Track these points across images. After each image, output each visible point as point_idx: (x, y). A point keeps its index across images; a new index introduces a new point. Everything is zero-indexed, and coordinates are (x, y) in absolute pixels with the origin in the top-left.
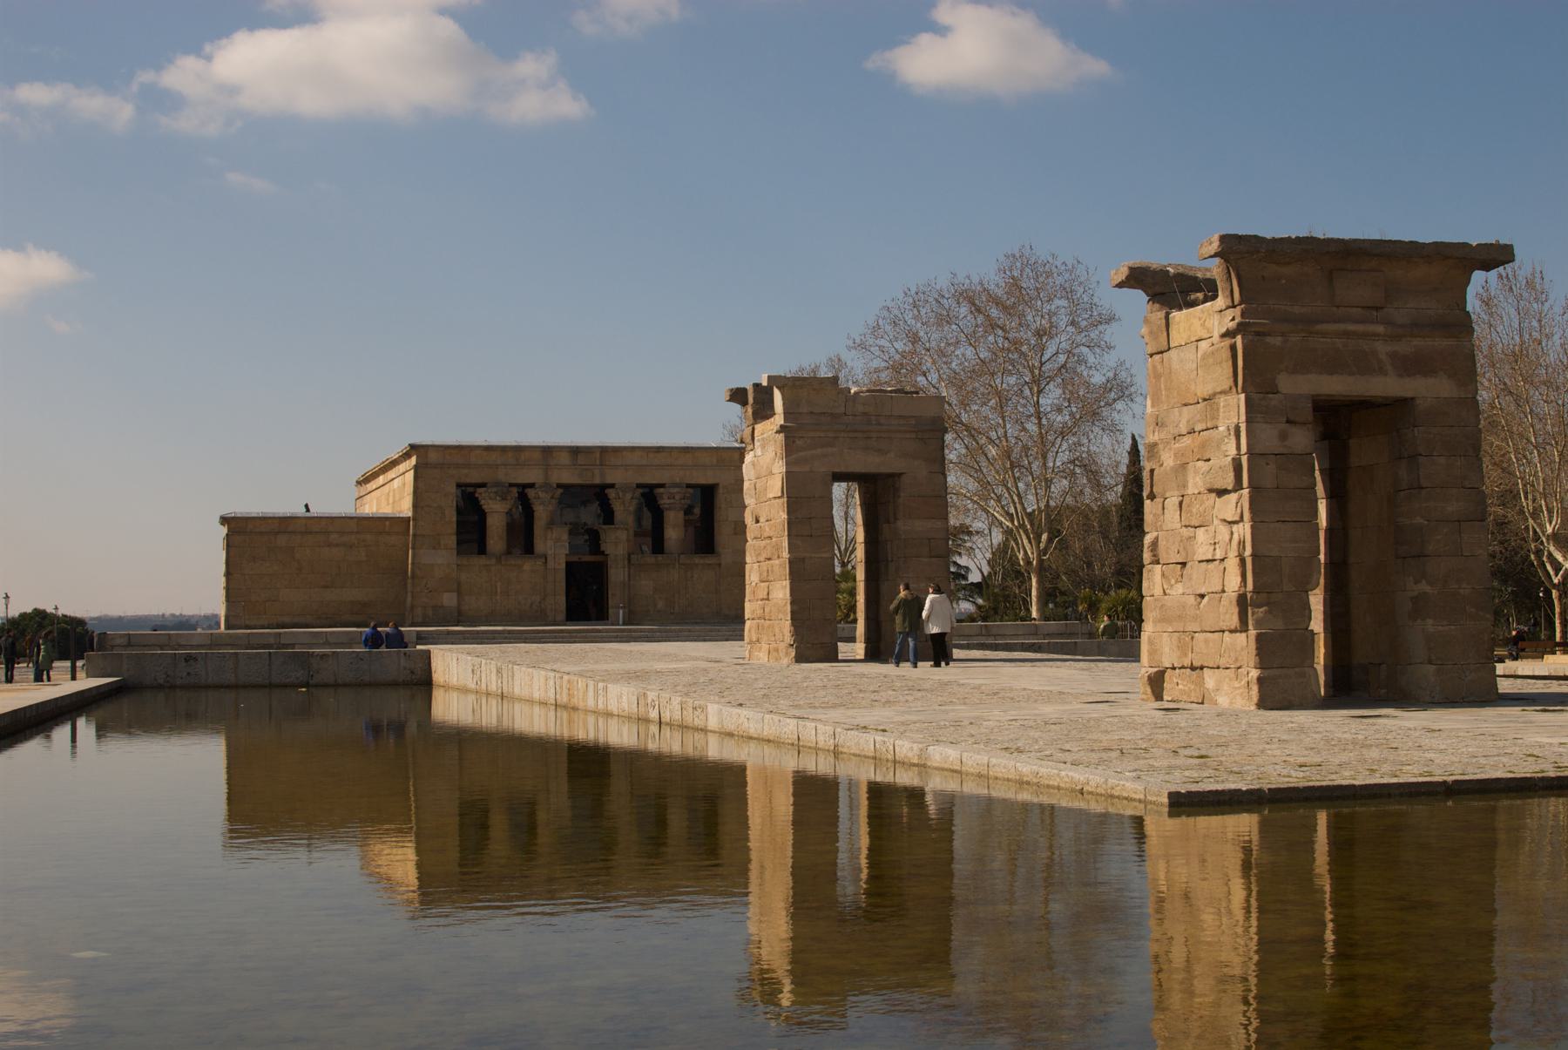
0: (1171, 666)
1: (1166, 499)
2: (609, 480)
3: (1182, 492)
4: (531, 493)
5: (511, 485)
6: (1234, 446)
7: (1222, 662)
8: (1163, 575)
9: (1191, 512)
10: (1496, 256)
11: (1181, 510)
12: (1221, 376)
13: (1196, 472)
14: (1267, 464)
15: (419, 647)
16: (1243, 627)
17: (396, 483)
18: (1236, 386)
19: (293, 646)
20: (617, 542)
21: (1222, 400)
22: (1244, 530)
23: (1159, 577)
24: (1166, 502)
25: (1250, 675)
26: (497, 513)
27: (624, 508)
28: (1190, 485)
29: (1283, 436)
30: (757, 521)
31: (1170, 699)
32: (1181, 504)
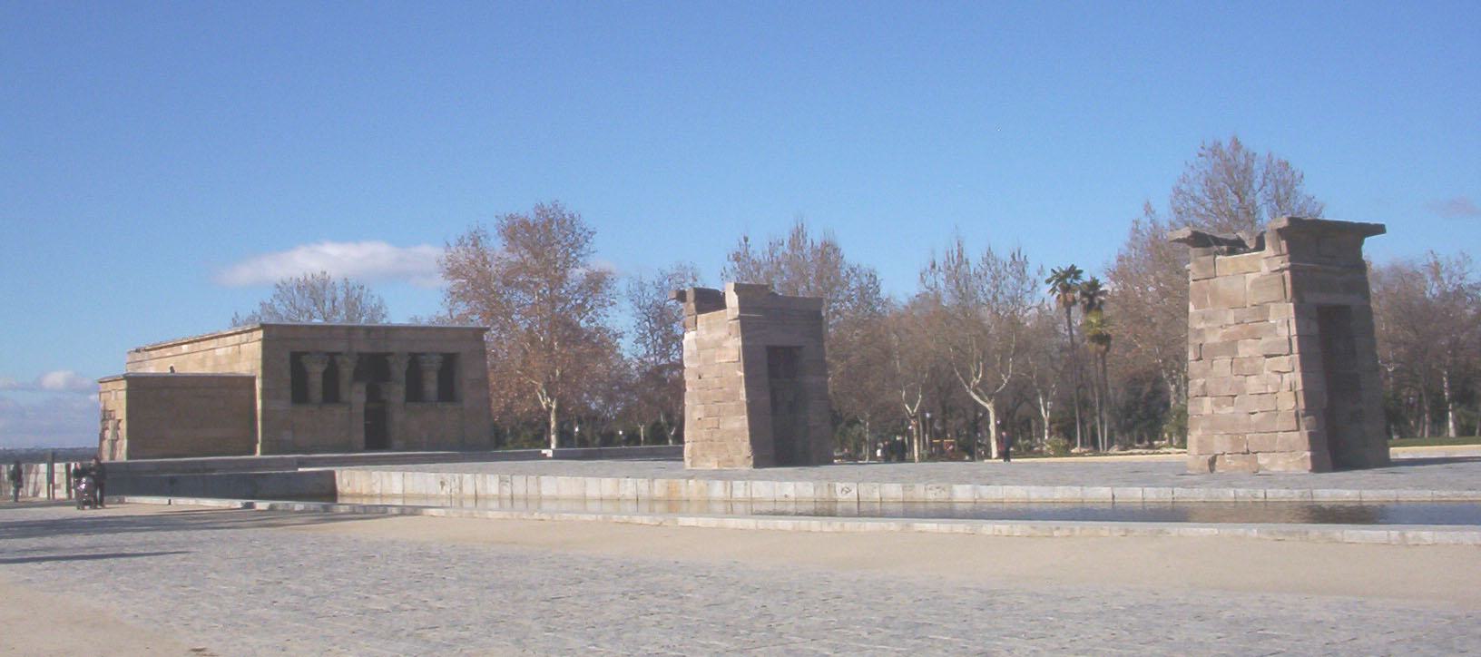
2: (391, 350)
4: (338, 359)
5: (328, 354)
7: (1277, 448)
10: (1379, 229)
12: (1276, 293)
15: (300, 470)
16: (1298, 430)
17: (219, 352)
18: (1286, 297)
19: (213, 470)
20: (396, 392)
21: (1272, 306)
22: (1297, 377)
26: (316, 371)
27: (399, 370)
30: (700, 378)
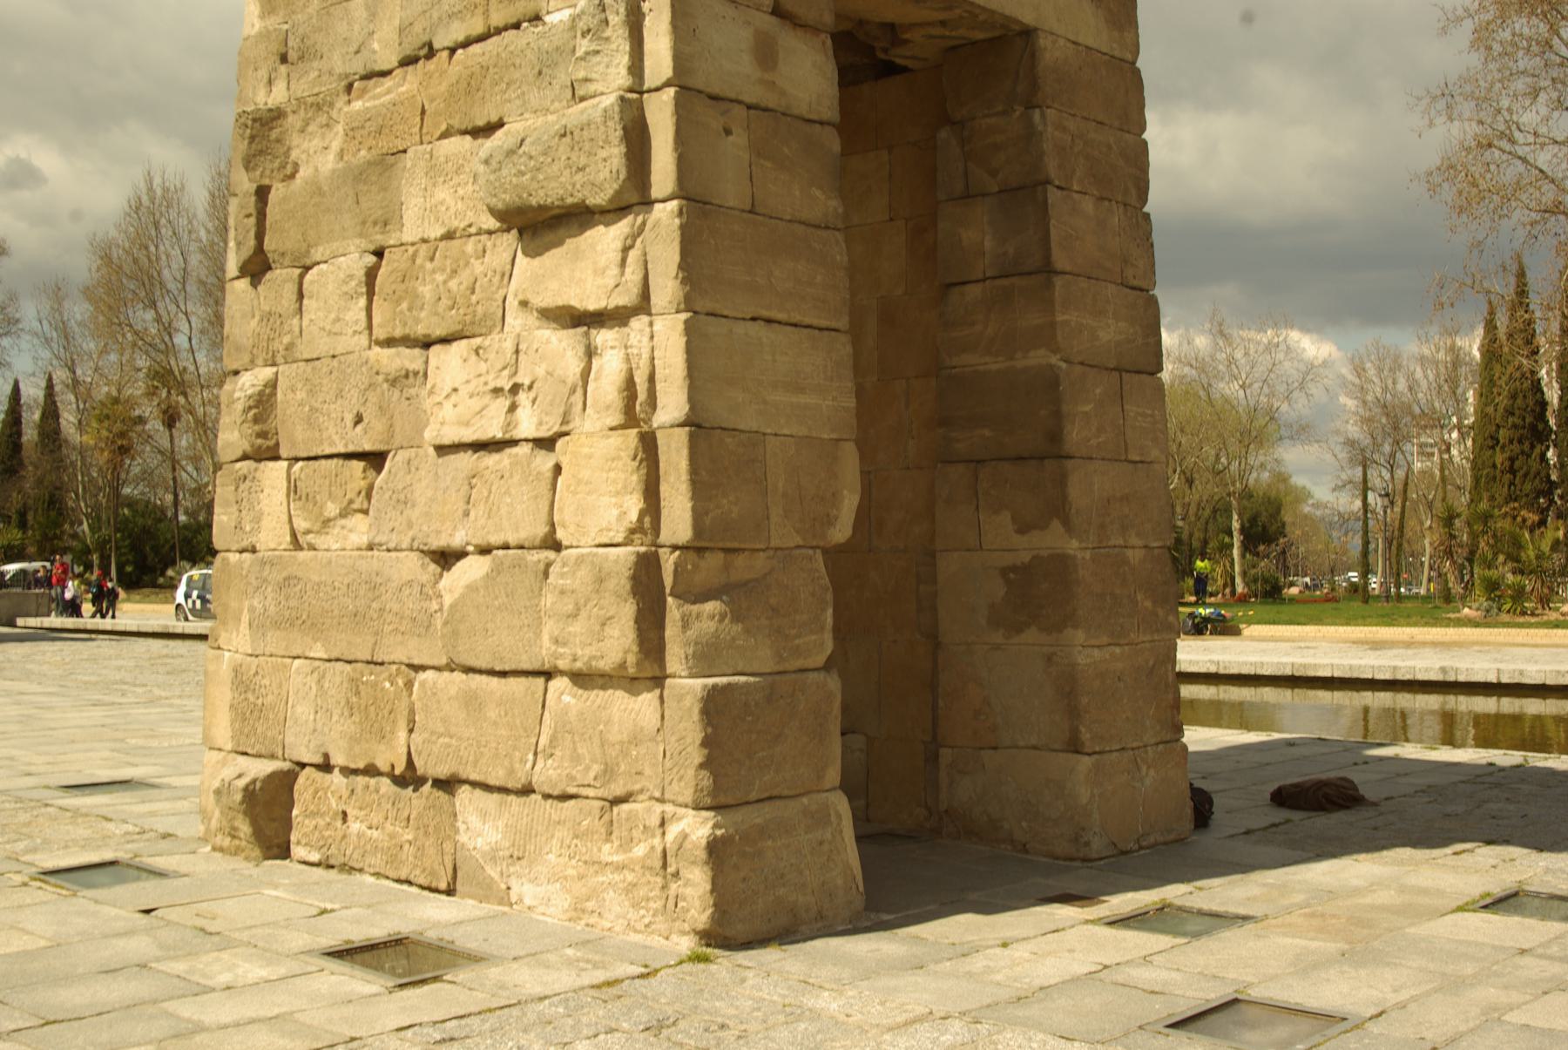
0: (318, 759)
1: (307, 268)
3: (379, 239)
6: (624, 60)
8: (293, 489)
9: (415, 296)
11: (371, 294)
13: (435, 171)
14: (728, 132)
23: (281, 495)
24: (309, 277)
25: (673, 831)
28: (410, 214)
29: (766, 54)
31: (315, 857)
32: (371, 275)
